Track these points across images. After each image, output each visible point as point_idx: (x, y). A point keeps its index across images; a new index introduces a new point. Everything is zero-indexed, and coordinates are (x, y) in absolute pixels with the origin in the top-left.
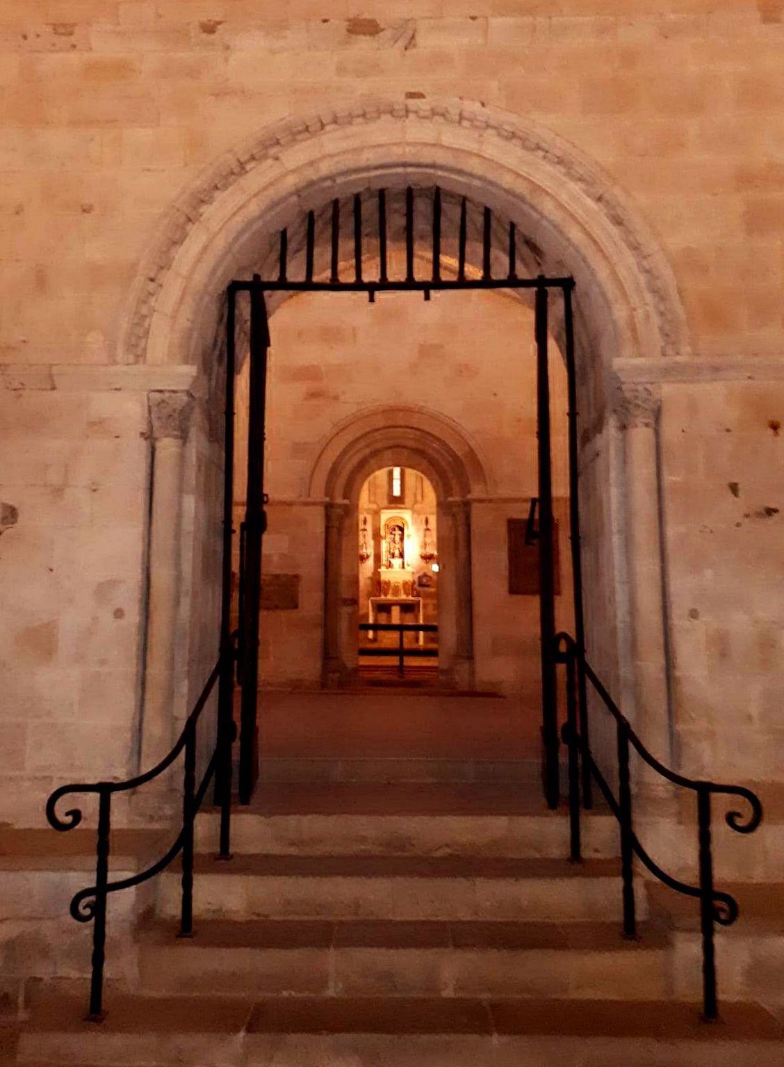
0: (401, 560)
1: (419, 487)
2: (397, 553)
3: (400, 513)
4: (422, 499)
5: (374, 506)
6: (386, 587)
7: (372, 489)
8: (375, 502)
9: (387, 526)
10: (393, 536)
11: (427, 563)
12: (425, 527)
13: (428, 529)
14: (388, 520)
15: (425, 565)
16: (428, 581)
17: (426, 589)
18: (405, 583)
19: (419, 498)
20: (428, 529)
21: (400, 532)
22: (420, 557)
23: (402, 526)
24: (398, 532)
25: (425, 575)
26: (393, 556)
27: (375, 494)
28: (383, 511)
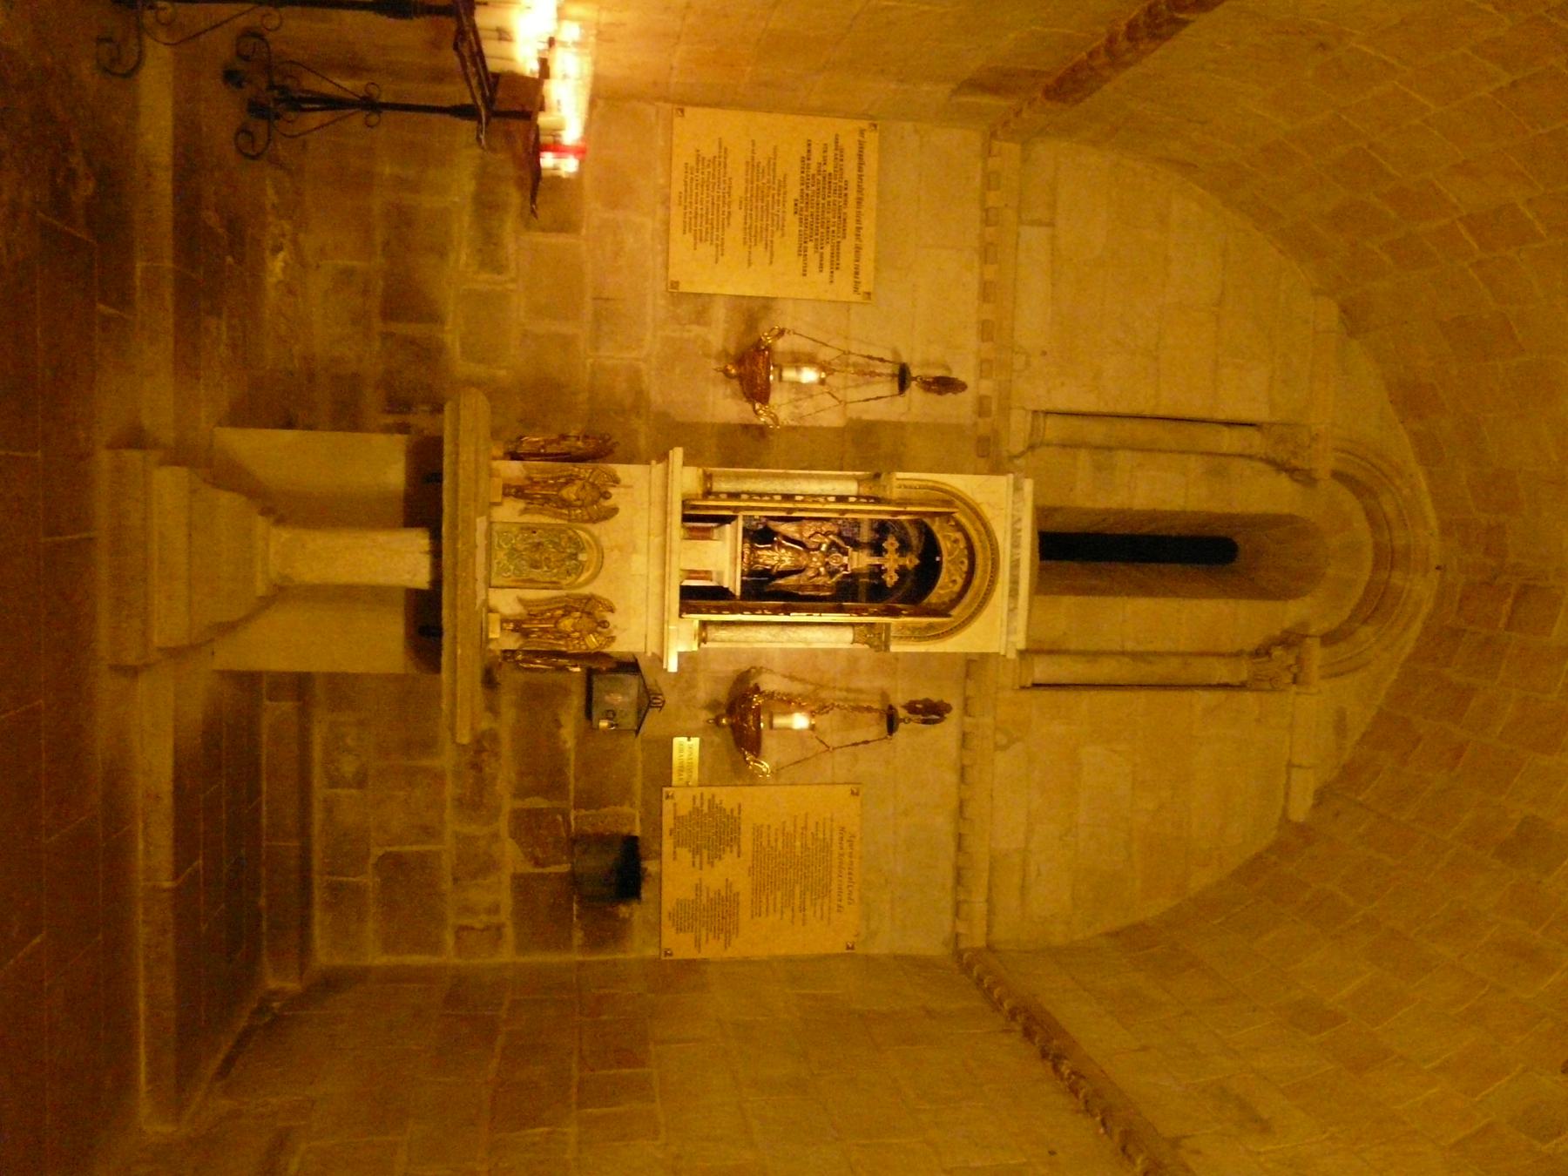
0: (732, 581)
1: (1105, 670)
2: (776, 558)
3: (1014, 593)
4: (1036, 686)
5: (1017, 431)
6: (570, 493)
7: (1097, 432)
8: (1032, 447)
9: (950, 498)
10: (865, 535)
11: (713, 706)
12: (899, 699)
13: (892, 723)
14: (977, 515)
15: (704, 691)
16: (610, 714)
17: (576, 701)
18: (592, 610)
19: (1043, 670)
20: (892, 723)
21: (891, 579)
22: (744, 667)
23: (933, 598)
24: (892, 562)
25: (649, 700)
26: (761, 535)
27: (1066, 445)
28: (1028, 485)
